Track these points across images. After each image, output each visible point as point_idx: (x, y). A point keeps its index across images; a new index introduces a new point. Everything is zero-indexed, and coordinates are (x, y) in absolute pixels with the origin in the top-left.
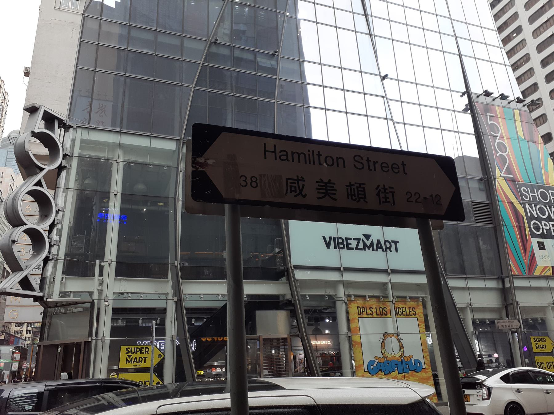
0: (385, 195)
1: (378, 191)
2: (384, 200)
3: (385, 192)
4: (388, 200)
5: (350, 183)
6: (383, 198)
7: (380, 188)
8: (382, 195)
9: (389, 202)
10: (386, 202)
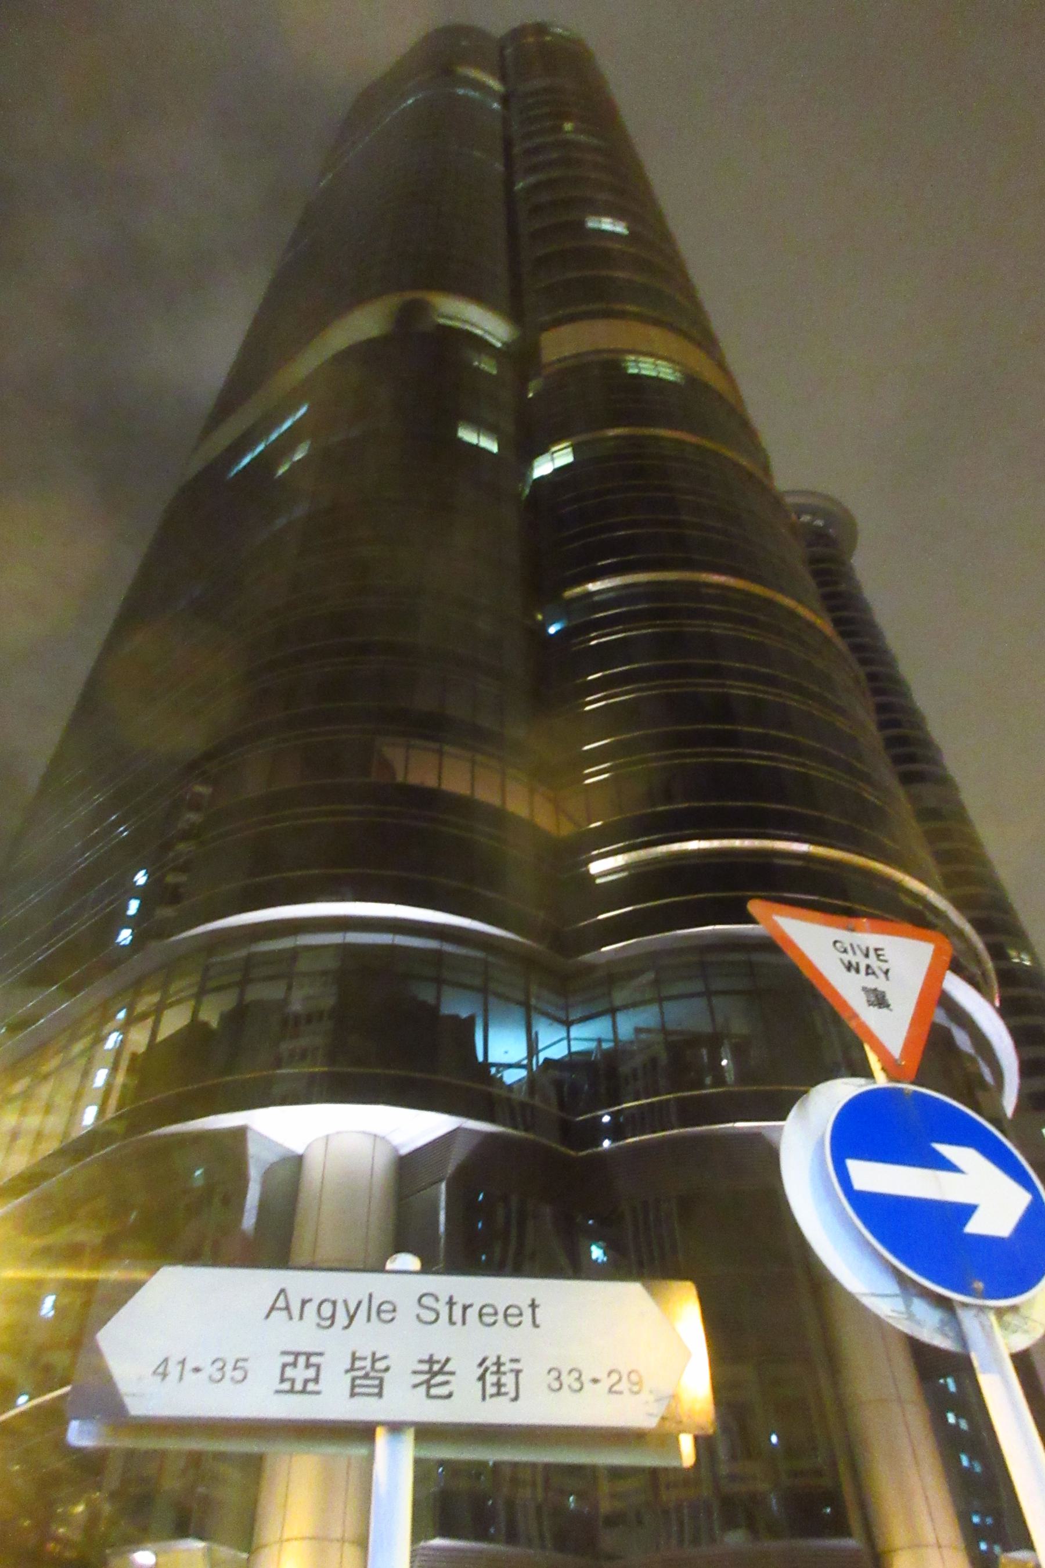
1: (481, 1370)
2: (494, 1390)
3: (498, 1372)
5: (431, 1356)
7: (488, 1363)
8: (491, 1379)
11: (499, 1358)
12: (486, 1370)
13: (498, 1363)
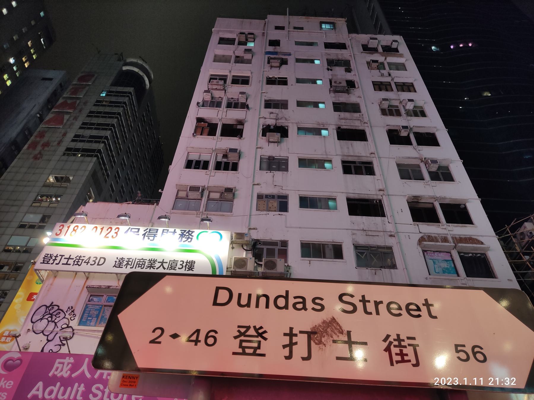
0: (401, 351)
2: (399, 358)
3: (400, 346)
4: (406, 358)
6: (397, 354)
7: (391, 339)
9: (409, 361)
10: (403, 361)
11: (398, 336)
12: (391, 343)
13: (398, 339)
